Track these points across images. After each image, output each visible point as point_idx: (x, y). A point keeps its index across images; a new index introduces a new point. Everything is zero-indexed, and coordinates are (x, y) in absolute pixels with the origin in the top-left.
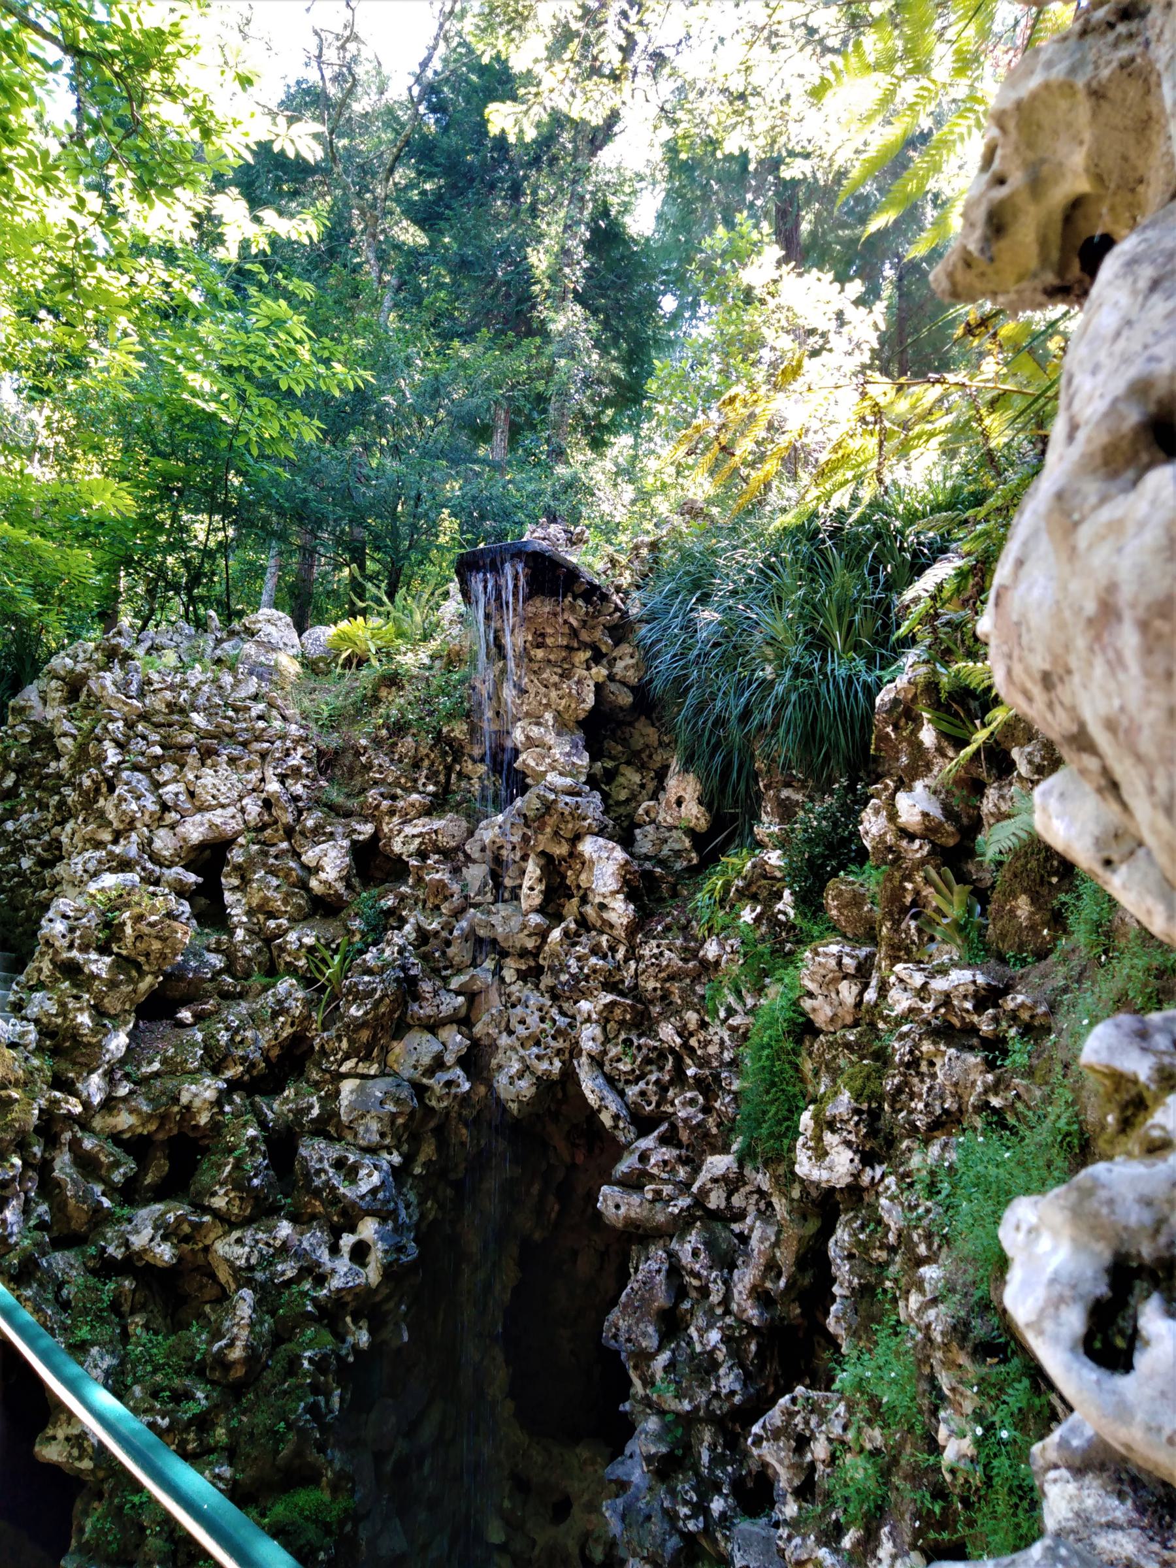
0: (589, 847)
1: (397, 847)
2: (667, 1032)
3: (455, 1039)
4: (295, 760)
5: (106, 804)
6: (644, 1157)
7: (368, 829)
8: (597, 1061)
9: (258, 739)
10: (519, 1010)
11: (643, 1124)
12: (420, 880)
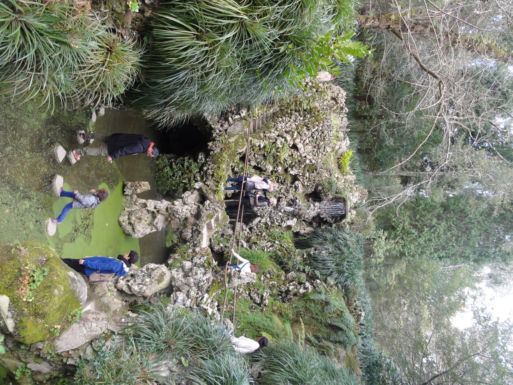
0: (295, 220)
1: (297, 182)
2: (264, 234)
4: (313, 161)
6: (245, 230)
7: (301, 174)
8: (260, 222)
11: (250, 229)
12: (291, 187)
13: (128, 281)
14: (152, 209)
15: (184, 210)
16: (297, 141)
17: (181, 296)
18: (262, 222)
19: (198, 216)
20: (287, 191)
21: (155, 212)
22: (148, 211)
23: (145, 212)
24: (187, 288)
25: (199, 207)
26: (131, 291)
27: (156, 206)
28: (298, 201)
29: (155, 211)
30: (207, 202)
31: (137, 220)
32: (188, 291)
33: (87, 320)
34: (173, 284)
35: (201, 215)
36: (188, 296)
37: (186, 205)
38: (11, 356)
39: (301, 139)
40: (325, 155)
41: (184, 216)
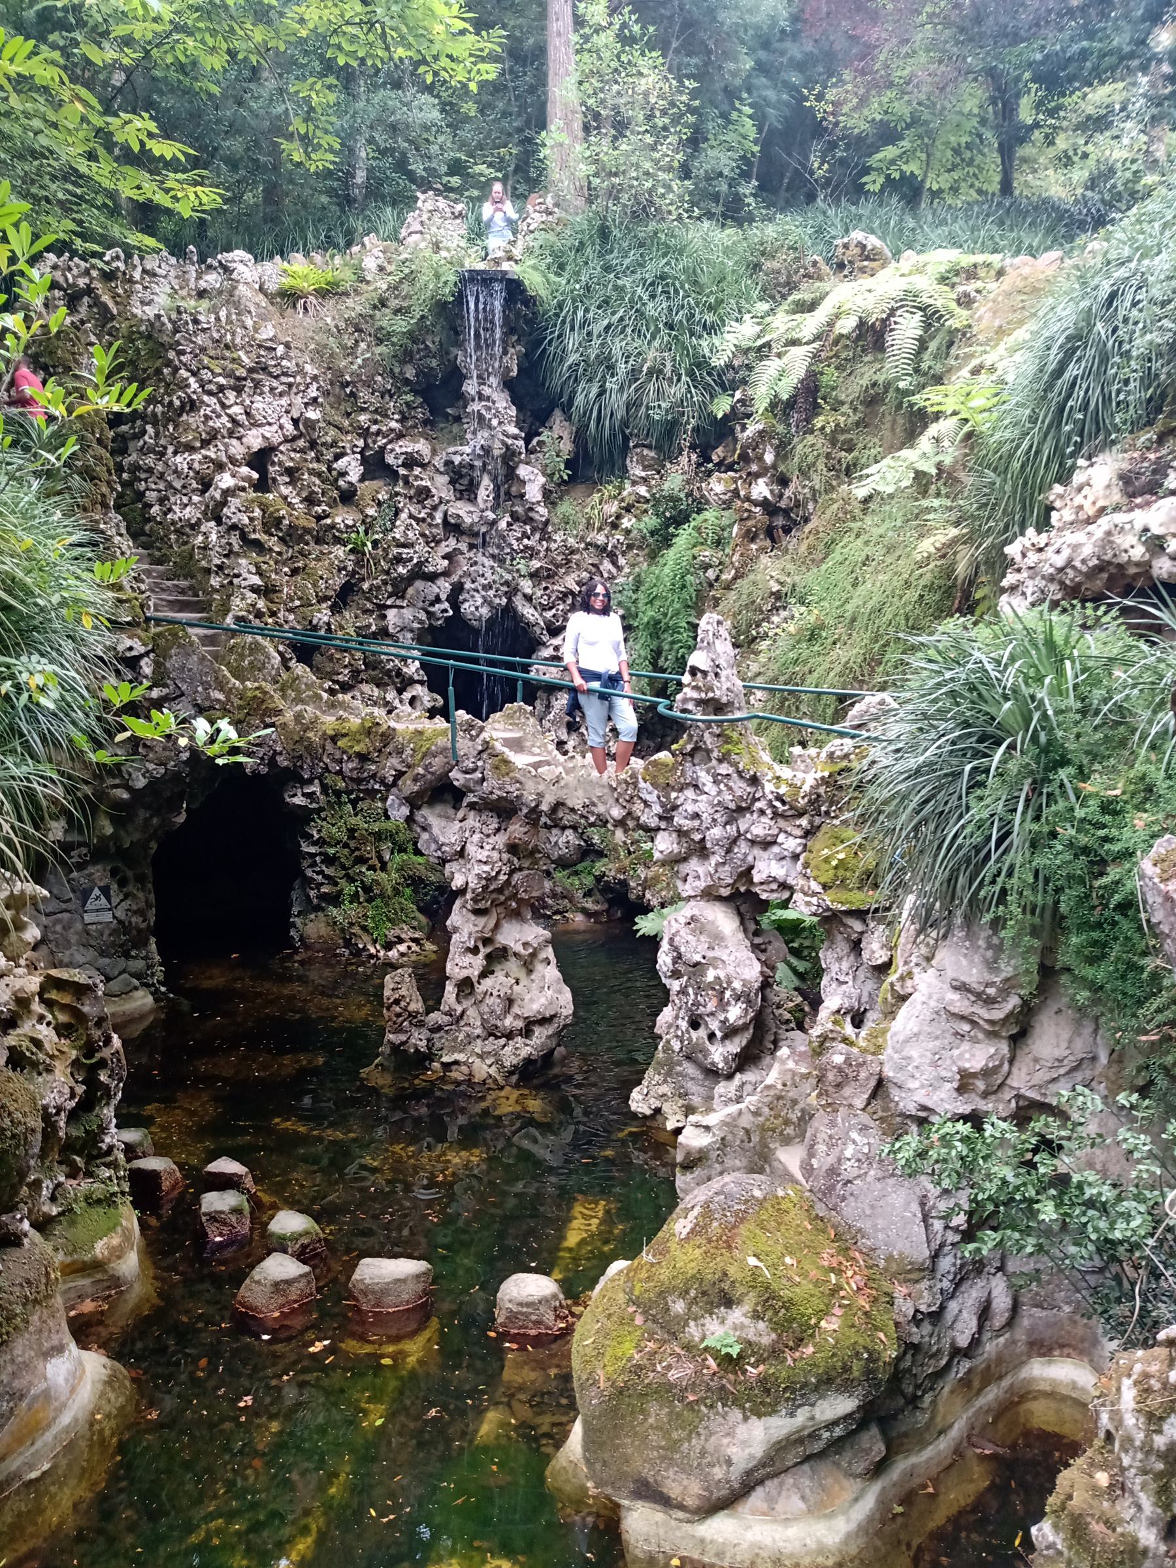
0: (523, 471)
1: (390, 459)
3: (444, 587)
4: (313, 392)
5: (193, 420)
7: (361, 443)
8: (528, 598)
9: (285, 374)
10: (479, 568)
12: (407, 482)
13: (712, 1036)
14: (479, 961)
15: (483, 855)
16: (237, 449)
17: (767, 867)
18: (529, 591)
19: (503, 810)
20: (423, 494)
21: (489, 950)
22: (484, 974)
23: (487, 983)
24: (742, 848)
25: (472, 806)
26: (745, 1027)
27: (468, 950)
28: (457, 460)
29: (484, 951)
30: (457, 777)
31: (516, 1010)
32: (753, 842)
33: (833, 1172)
34: (725, 892)
35: (500, 798)
36: (766, 844)
37: (473, 851)
38: (928, 1398)
39: (231, 433)
40: (287, 346)
41: (505, 856)
